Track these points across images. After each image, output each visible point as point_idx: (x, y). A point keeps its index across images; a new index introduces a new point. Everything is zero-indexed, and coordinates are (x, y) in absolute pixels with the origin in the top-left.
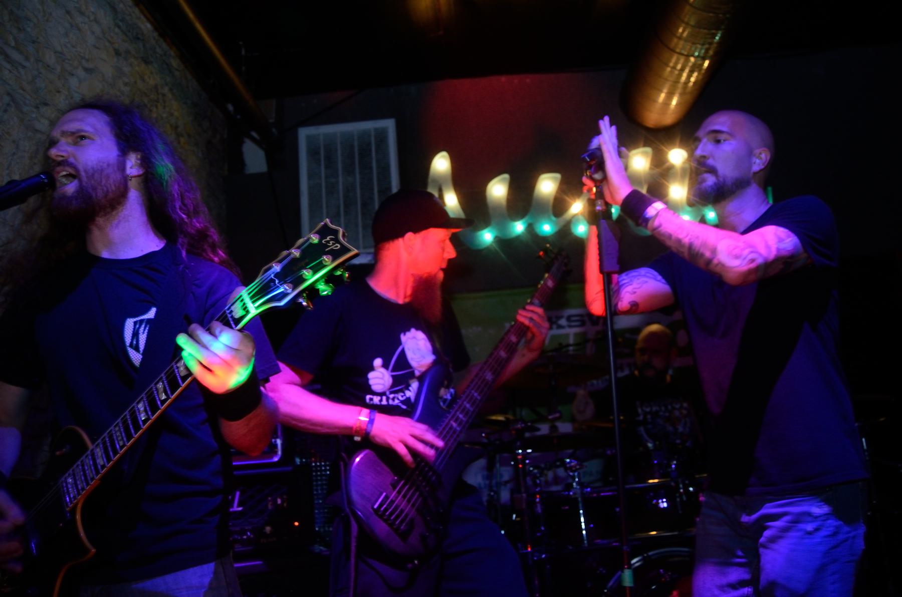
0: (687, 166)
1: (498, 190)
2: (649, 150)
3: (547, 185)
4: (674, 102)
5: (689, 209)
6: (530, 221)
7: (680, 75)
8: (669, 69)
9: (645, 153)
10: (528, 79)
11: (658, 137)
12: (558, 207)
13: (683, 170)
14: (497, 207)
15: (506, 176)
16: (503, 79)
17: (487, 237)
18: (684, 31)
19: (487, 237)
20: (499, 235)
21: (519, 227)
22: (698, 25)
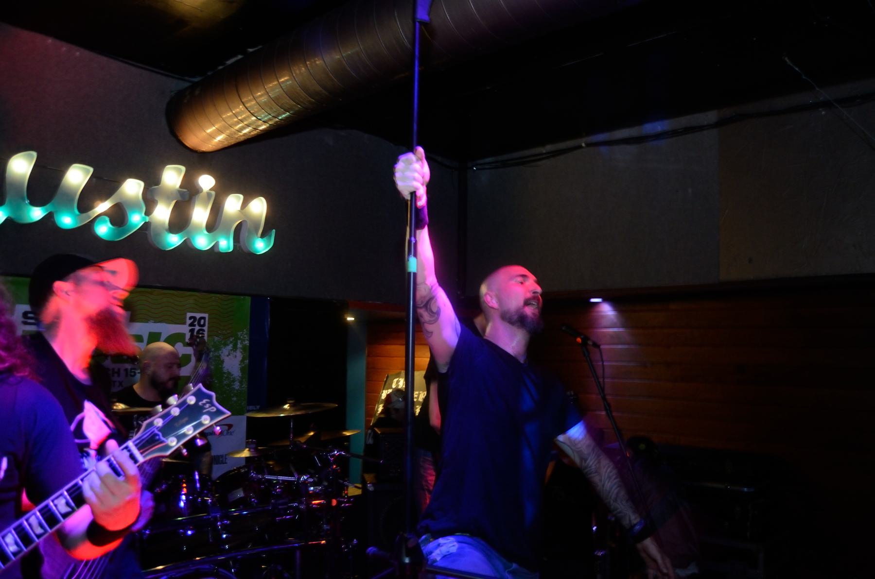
0: (213, 193)
2: (183, 168)
3: (77, 176)
4: (220, 138)
7: (238, 123)
8: (230, 114)
9: (180, 171)
10: (78, 53)
11: (196, 161)
13: (209, 195)
14: (16, 186)
16: (50, 40)
18: (261, 96)
20: (13, 216)
21: (36, 214)
22: (276, 100)
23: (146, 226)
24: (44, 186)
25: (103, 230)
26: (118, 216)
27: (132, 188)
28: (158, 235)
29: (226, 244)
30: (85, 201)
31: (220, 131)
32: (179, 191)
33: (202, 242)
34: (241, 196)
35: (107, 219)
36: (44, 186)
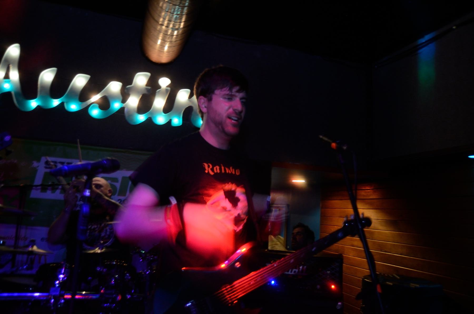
0: (169, 88)
1: (47, 76)
2: (149, 74)
3: (80, 81)
5: (164, 114)
6: (64, 101)
12: (83, 96)
13: (167, 90)
15: (55, 69)
17: (33, 104)
19: (33, 104)
21: (55, 103)
23: (122, 110)
24: (60, 87)
25: (95, 113)
26: (105, 104)
27: (115, 87)
28: (131, 115)
29: (177, 121)
30: (83, 96)
31: (162, 46)
32: (147, 89)
33: (161, 120)
34: (189, 90)
35: (97, 105)
36: (60, 87)
